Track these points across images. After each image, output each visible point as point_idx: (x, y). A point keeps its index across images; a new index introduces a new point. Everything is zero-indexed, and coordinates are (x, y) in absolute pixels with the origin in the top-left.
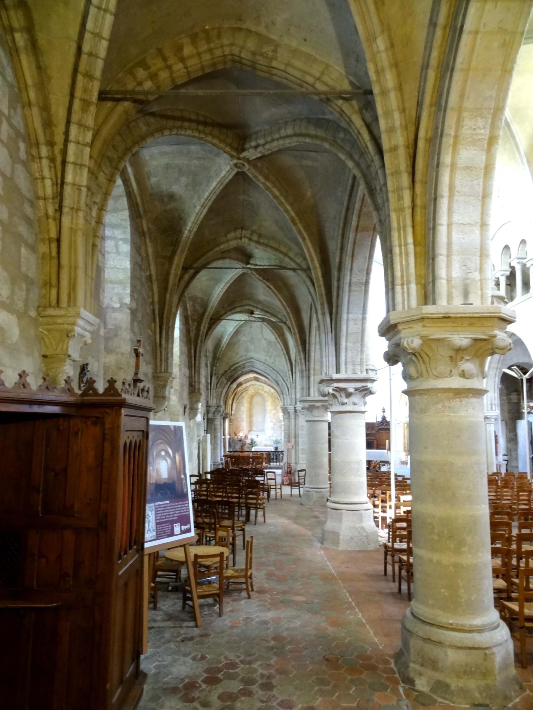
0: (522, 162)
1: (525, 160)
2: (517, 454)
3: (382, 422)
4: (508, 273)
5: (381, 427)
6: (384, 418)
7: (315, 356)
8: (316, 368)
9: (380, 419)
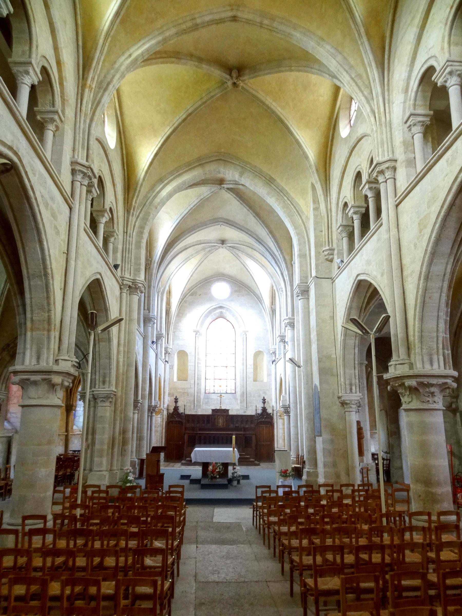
0: (359, 34)
1: (362, 30)
2: (400, 452)
3: (262, 414)
4: (363, 210)
5: (261, 420)
6: (264, 409)
7: (31, 298)
8: (34, 318)
9: (260, 411)
